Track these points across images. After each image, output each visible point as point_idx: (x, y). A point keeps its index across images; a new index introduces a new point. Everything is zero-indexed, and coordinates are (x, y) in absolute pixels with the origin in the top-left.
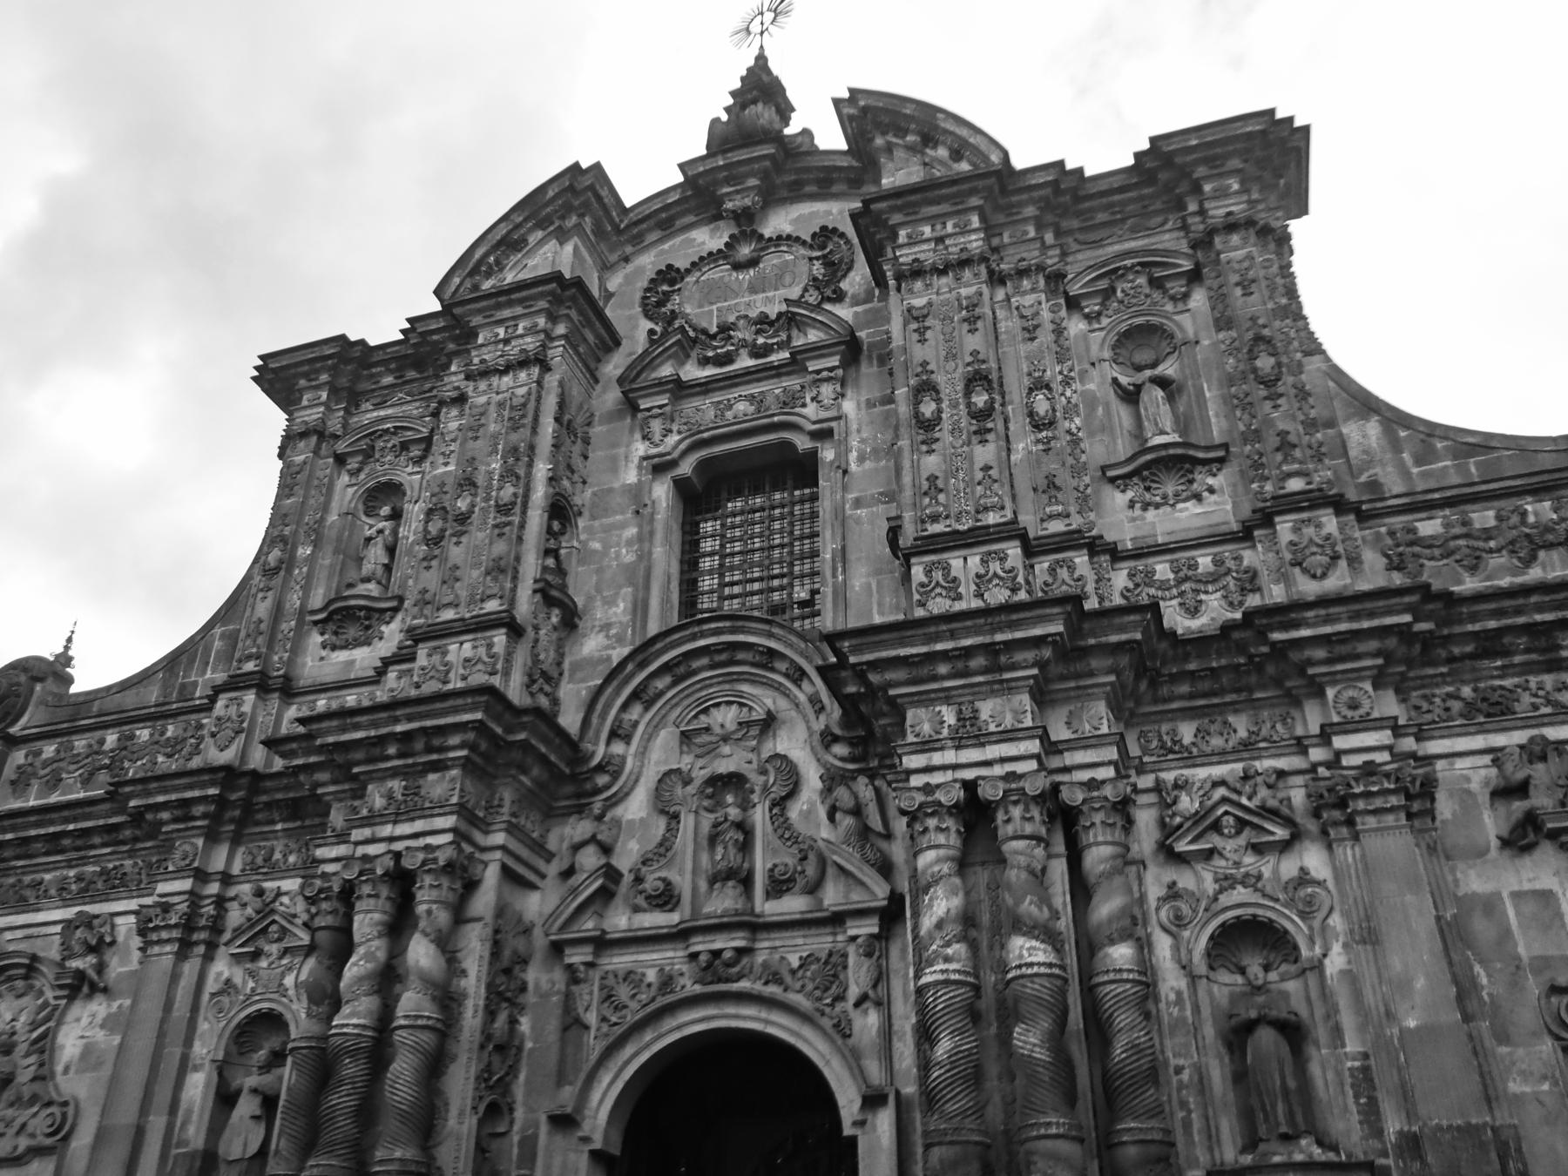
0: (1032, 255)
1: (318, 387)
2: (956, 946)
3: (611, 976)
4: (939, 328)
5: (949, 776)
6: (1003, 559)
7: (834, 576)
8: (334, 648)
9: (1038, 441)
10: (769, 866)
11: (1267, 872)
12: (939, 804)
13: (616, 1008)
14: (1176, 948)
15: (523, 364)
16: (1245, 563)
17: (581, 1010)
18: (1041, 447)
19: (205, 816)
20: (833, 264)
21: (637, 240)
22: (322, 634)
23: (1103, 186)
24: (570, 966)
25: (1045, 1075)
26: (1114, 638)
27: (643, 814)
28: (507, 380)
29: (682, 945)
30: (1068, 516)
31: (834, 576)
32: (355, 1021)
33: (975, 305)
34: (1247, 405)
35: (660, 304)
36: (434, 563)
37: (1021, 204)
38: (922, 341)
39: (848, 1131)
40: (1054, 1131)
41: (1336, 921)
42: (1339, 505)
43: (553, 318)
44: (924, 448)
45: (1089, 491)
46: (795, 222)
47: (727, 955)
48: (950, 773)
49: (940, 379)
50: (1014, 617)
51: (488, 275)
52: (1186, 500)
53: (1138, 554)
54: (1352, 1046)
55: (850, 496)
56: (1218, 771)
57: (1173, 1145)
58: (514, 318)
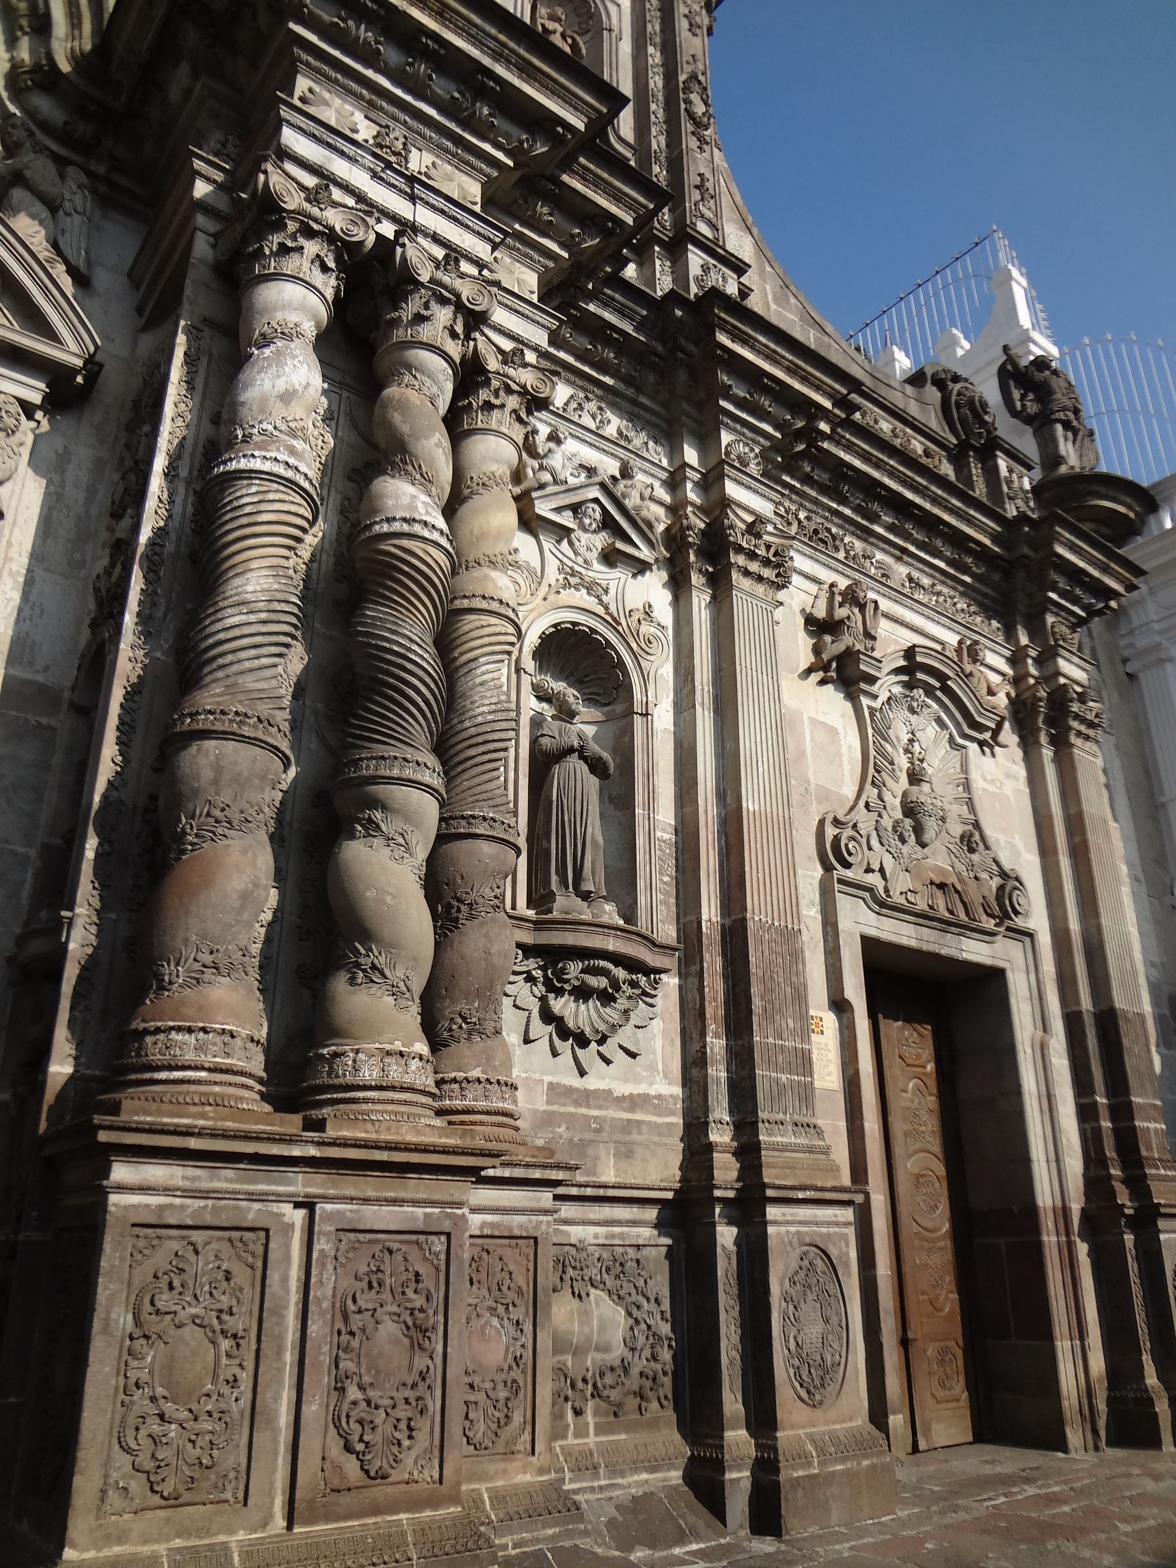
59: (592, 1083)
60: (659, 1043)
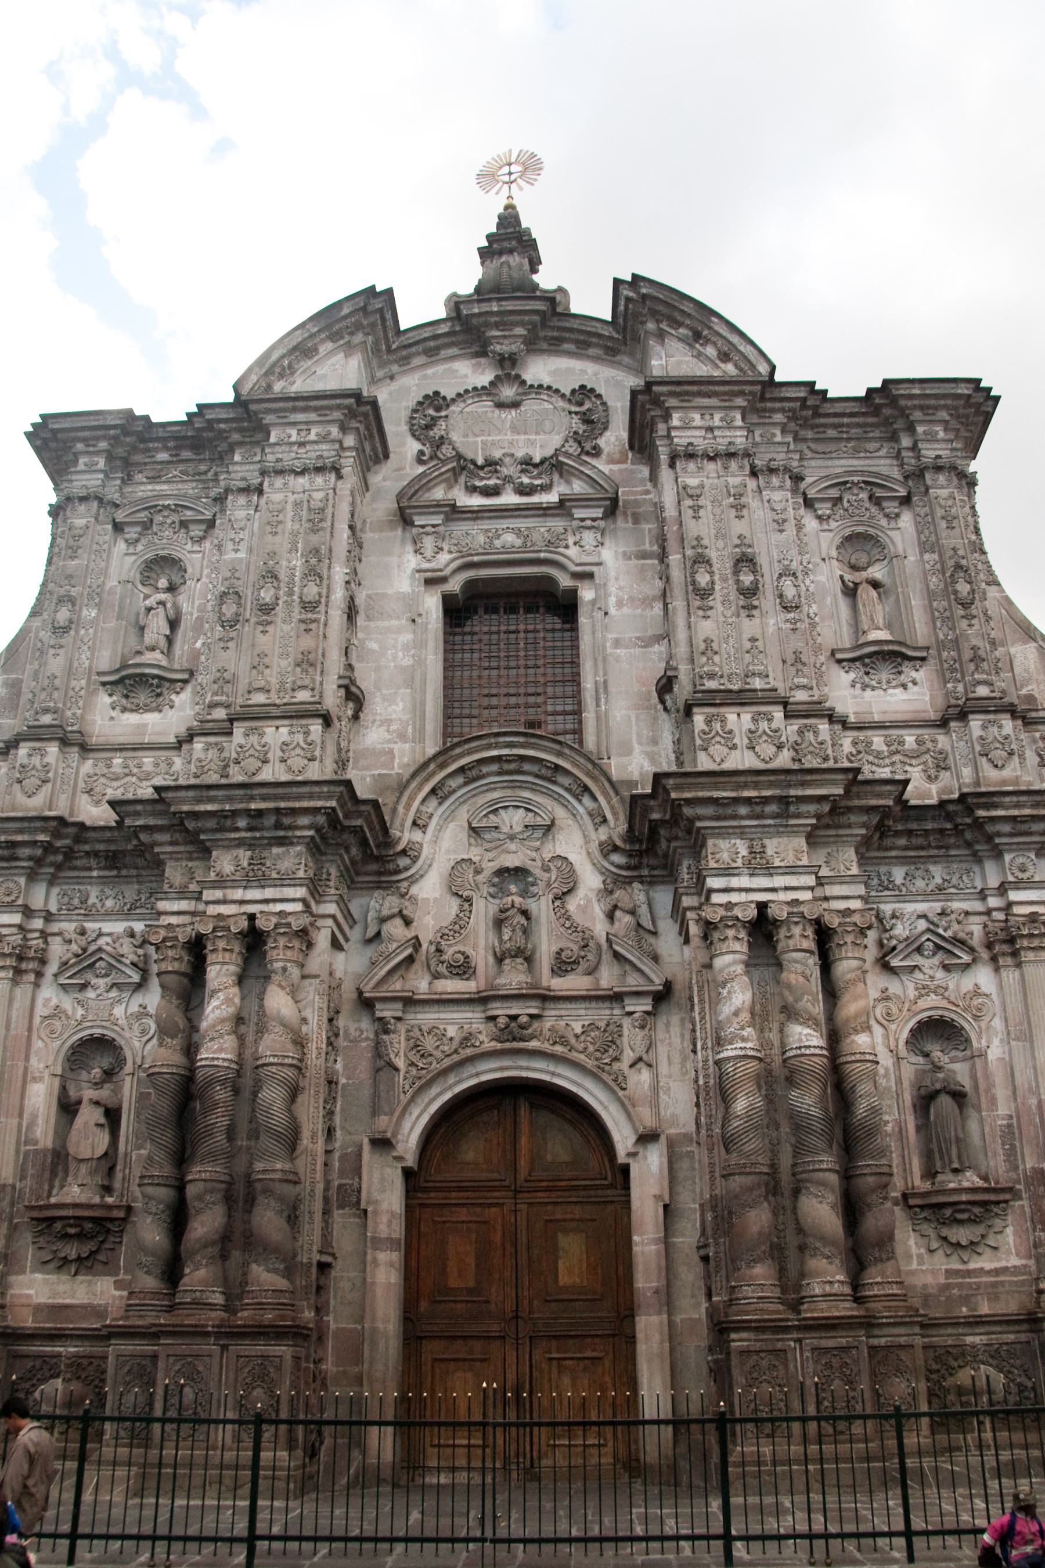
0: (780, 458)
1: (97, 453)
2: (749, 1030)
3: (416, 1030)
4: (709, 508)
5: (742, 897)
6: (770, 720)
7: (598, 705)
8: (124, 710)
9: (787, 621)
10: (554, 948)
11: (951, 987)
12: (737, 919)
13: (422, 1056)
14: (886, 1036)
15: (319, 470)
16: (940, 746)
17: (392, 1056)
18: (789, 626)
19: (30, 858)
20: (592, 422)
21: (405, 361)
22: (110, 695)
23: (839, 408)
24: (381, 1019)
25: (818, 1126)
26: (873, 802)
27: (437, 895)
28: (302, 481)
29: (482, 1008)
30: (811, 688)
31: (598, 705)
32: (223, 1056)
33: (741, 495)
34: (949, 621)
35: (428, 427)
36: (231, 645)
37: (773, 411)
38: (697, 518)
39: (621, 1158)
40: (824, 1166)
41: (997, 1023)
42: (1012, 711)
43: (343, 429)
44: (701, 613)
45: (824, 668)
46: (553, 373)
47: (524, 1019)
48: (743, 894)
49: (713, 555)
50: (808, 778)
51: (281, 376)
52: (895, 687)
53: (860, 728)
54: (1003, 1108)
55: (610, 636)
56: (921, 907)
57: (891, 1175)
58: (307, 423)
59: (972, 1266)
60: (1011, 1239)
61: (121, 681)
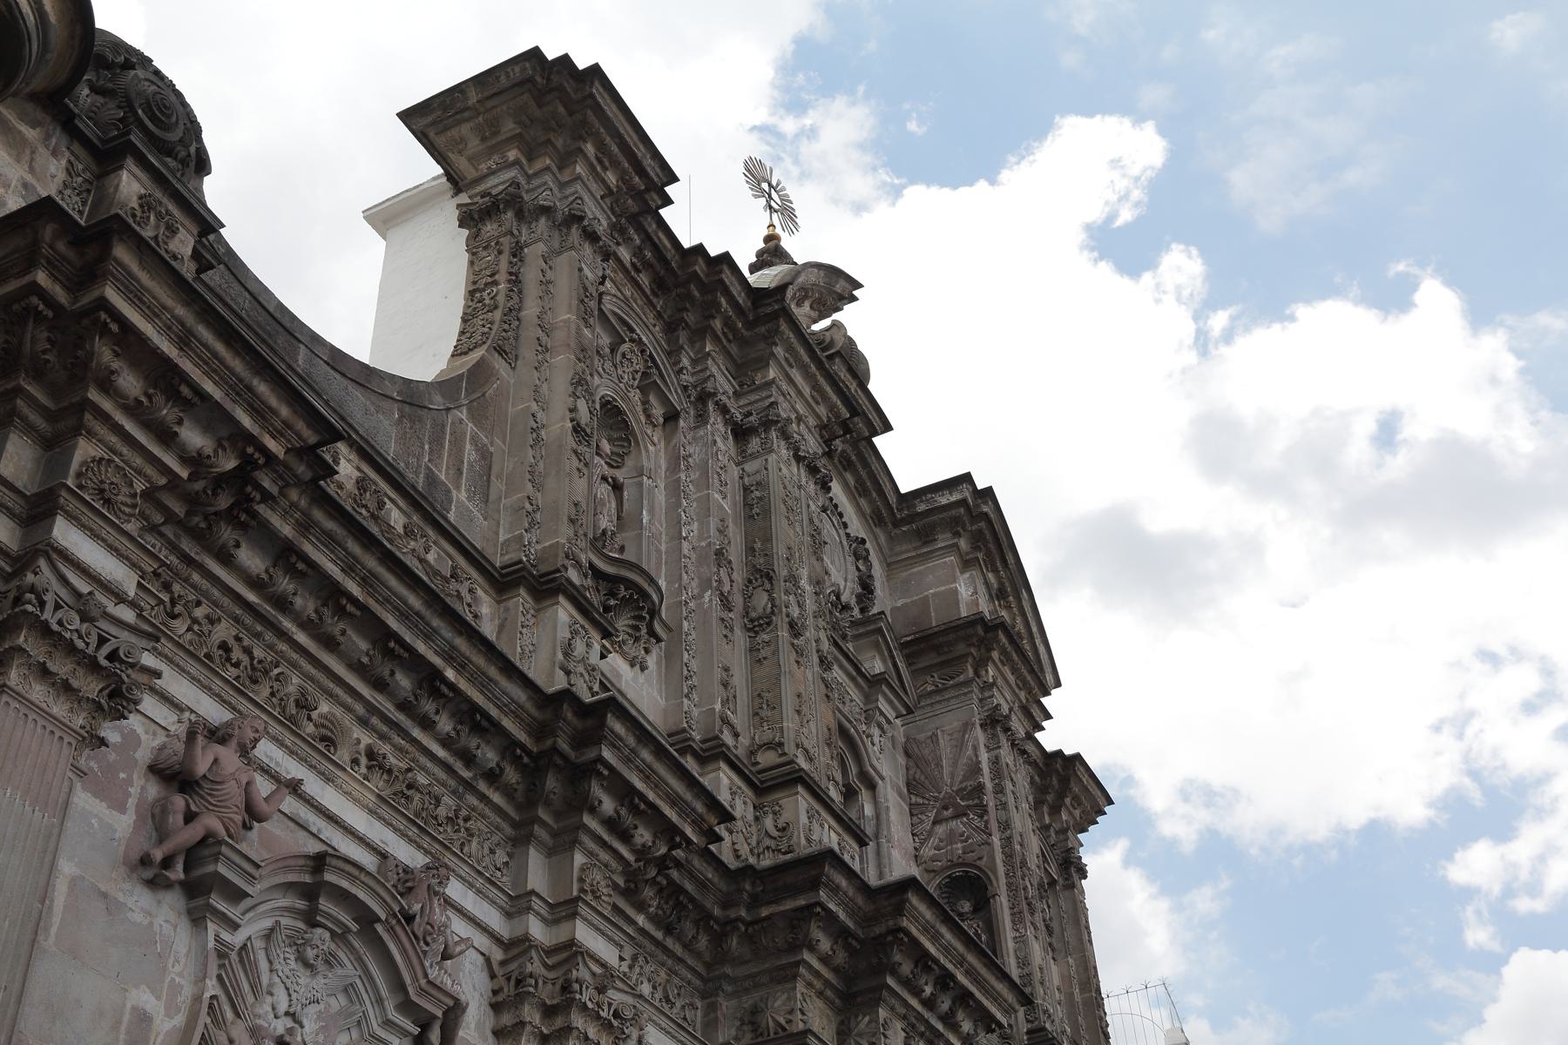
61: (614, 580)
